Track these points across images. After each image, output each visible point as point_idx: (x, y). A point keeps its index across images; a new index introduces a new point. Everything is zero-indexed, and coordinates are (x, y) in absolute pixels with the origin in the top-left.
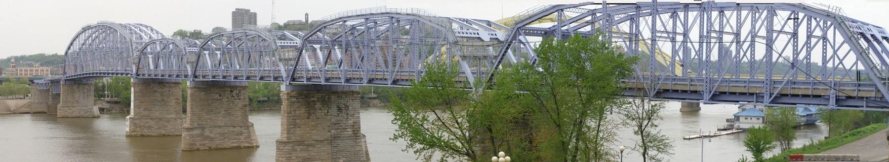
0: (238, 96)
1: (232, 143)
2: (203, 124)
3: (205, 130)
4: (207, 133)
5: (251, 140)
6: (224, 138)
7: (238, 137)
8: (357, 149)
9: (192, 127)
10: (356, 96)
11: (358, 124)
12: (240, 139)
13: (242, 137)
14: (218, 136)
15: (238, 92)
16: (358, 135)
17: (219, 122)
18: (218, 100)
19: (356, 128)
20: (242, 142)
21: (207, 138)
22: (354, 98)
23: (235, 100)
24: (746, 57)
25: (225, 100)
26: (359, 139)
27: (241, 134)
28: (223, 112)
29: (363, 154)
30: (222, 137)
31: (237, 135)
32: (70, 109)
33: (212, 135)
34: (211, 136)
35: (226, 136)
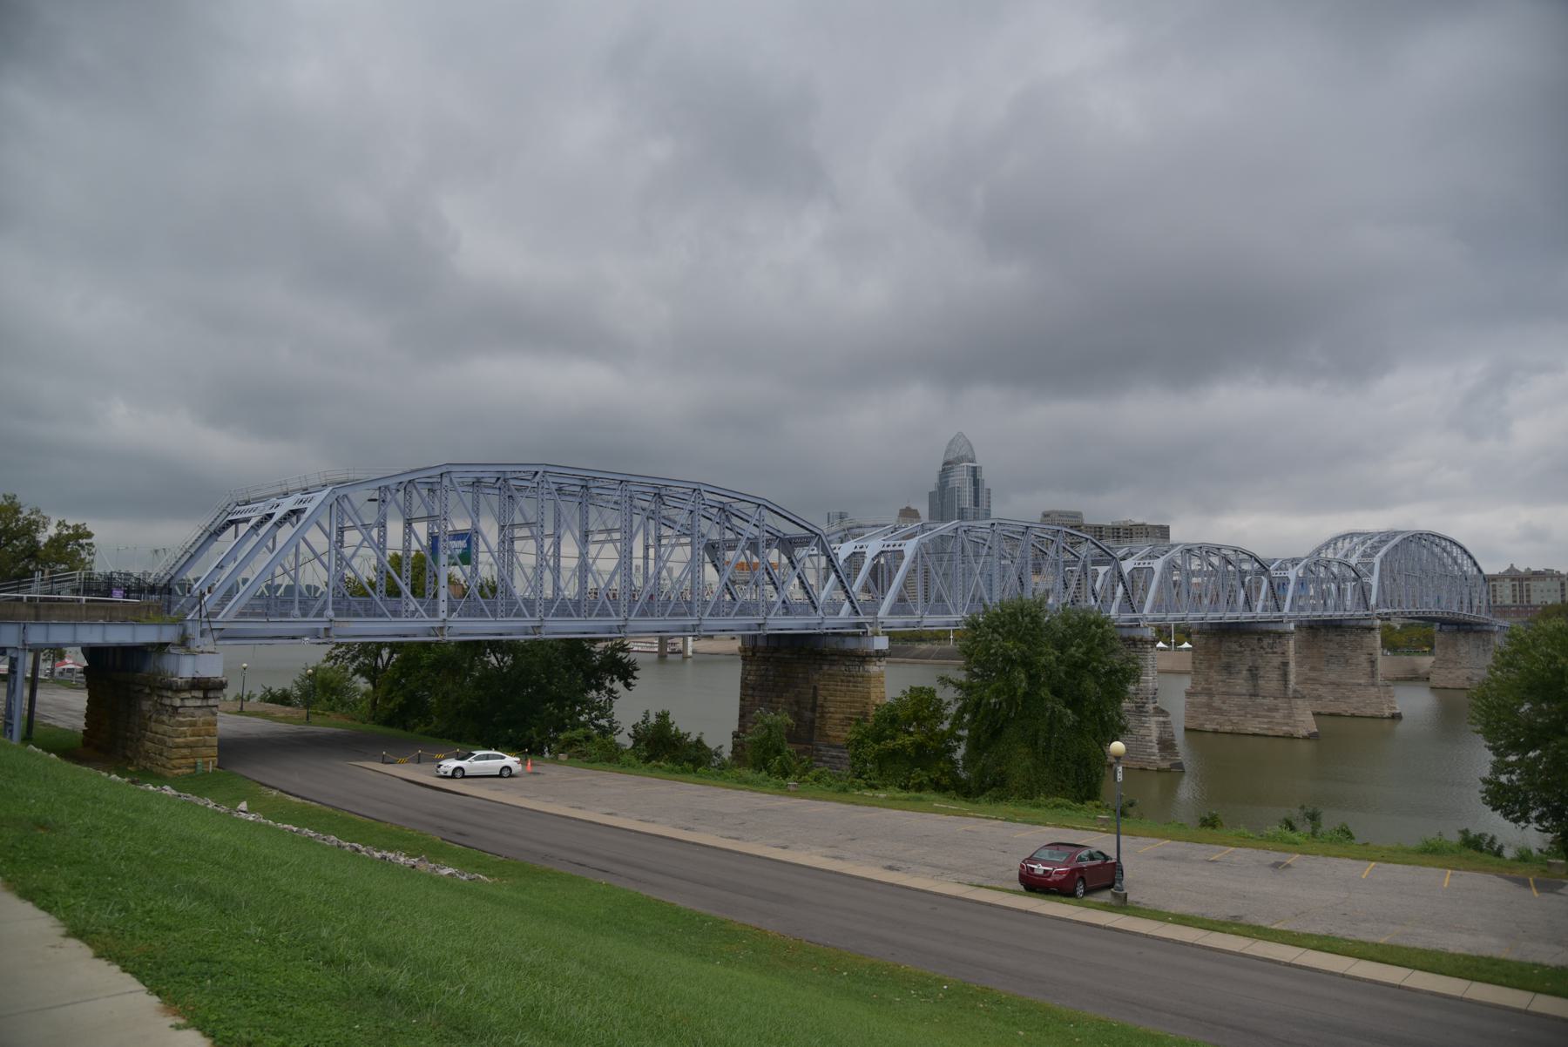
0: (1272, 648)
1: (1260, 723)
2: (1210, 689)
3: (1214, 698)
4: (1217, 702)
5: (1295, 721)
6: (1246, 713)
7: (1269, 714)
8: (1143, 732)
9: (1193, 691)
10: (1141, 646)
11: (1144, 692)
12: (1274, 717)
13: (1278, 716)
14: (1236, 709)
15: (1271, 642)
16: (1145, 710)
17: (1238, 687)
18: (1237, 652)
19: (1141, 699)
20: (1278, 723)
21: (1220, 712)
22: (1137, 650)
23: (1266, 653)
24: (601, 549)
25: (1247, 653)
26: (1146, 717)
27: (1276, 709)
28: (1244, 672)
29: (1151, 742)
30: (1242, 712)
31: (1269, 710)
32: (1450, 673)
33: (1225, 707)
34: (1225, 708)
35: (1248, 710)
